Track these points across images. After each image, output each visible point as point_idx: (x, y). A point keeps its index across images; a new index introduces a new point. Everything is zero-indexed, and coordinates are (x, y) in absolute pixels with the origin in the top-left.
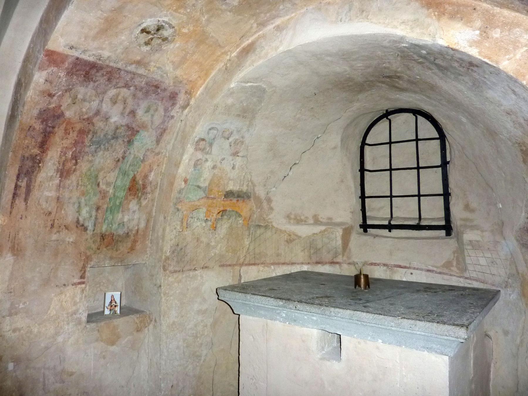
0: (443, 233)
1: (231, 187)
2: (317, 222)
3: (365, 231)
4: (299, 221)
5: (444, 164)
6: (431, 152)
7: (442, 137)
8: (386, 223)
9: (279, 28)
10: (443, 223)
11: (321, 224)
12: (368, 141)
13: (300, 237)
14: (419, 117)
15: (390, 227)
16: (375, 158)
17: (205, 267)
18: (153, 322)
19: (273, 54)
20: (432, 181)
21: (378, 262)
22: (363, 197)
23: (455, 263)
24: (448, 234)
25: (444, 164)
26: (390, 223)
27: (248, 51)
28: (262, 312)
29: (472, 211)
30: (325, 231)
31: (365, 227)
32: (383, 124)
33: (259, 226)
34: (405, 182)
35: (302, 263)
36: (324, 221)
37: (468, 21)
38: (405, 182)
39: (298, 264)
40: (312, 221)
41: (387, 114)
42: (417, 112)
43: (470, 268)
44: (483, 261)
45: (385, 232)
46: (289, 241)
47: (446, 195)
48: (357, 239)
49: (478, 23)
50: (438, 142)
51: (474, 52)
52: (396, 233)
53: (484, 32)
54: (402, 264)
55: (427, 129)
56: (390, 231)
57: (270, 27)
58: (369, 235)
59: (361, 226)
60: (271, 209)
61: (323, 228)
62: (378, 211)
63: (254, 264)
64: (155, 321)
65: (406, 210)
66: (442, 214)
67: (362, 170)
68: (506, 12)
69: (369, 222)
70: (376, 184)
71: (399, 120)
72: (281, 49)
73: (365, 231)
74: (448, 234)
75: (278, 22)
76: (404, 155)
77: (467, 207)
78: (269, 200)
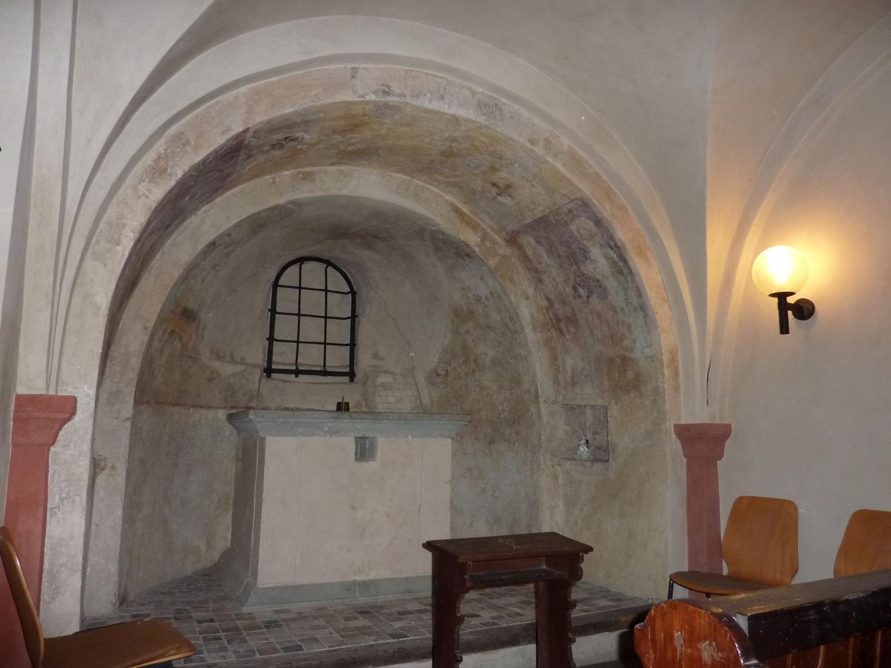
0: (347, 379)
1: (191, 305)
2: (233, 360)
3: (269, 376)
4: (220, 358)
5: (354, 317)
6: (341, 306)
7: (353, 293)
8: (294, 368)
9: (341, 172)
10: (347, 370)
11: (237, 363)
12: (280, 283)
13: (219, 375)
14: (330, 269)
15: (297, 372)
16: (286, 300)
17: (148, 402)
18: (106, 471)
19: (334, 192)
20: (340, 332)
21: (291, 406)
22: (271, 339)
23: (364, 404)
24: (352, 380)
25: (354, 317)
26: (297, 368)
27: (307, 177)
28: (300, 430)
29: (382, 359)
30: (244, 371)
31: (269, 371)
32: (294, 269)
33: (190, 357)
34: (312, 329)
35: (219, 408)
36: (239, 360)
37: (476, 232)
38: (312, 329)
39: (214, 408)
40: (229, 360)
41: (301, 260)
42: (328, 263)
43: (380, 406)
44: (391, 400)
45: (292, 377)
46: (210, 380)
47: (353, 345)
48: (268, 385)
49: (480, 234)
50: (350, 295)
51: (477, 250)
52: (302, 378)
53: (483, 240)
54: (315, 408)
55: (337, 282)
56: (297, 376)
57: (334, 168)
58: (275, 379)
59: (265, 371)
60: (203, 337)
61: (240, 368)
62: (284, 356)
63: (178, 405)
64: (113, 468)
65: (311, 357)
66: (348, 363)
67: (273, 311)
68: (493, 234)
69: (274, 367)
70: (285, 328)
71: (308, 266)
72: (345, 192)
73: (269, 376)
74: (352, 380)
75: (344, 168)
76: (312, 302)
77: (376, 356)
78: (204, 328)
